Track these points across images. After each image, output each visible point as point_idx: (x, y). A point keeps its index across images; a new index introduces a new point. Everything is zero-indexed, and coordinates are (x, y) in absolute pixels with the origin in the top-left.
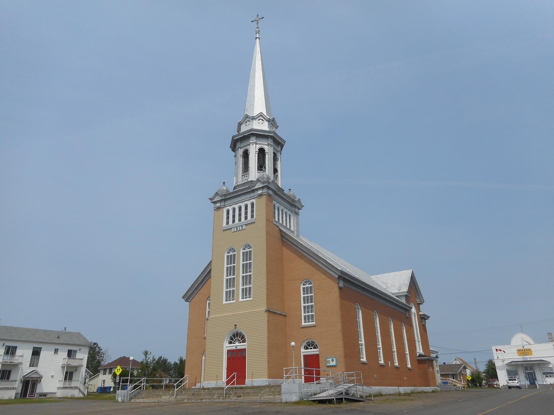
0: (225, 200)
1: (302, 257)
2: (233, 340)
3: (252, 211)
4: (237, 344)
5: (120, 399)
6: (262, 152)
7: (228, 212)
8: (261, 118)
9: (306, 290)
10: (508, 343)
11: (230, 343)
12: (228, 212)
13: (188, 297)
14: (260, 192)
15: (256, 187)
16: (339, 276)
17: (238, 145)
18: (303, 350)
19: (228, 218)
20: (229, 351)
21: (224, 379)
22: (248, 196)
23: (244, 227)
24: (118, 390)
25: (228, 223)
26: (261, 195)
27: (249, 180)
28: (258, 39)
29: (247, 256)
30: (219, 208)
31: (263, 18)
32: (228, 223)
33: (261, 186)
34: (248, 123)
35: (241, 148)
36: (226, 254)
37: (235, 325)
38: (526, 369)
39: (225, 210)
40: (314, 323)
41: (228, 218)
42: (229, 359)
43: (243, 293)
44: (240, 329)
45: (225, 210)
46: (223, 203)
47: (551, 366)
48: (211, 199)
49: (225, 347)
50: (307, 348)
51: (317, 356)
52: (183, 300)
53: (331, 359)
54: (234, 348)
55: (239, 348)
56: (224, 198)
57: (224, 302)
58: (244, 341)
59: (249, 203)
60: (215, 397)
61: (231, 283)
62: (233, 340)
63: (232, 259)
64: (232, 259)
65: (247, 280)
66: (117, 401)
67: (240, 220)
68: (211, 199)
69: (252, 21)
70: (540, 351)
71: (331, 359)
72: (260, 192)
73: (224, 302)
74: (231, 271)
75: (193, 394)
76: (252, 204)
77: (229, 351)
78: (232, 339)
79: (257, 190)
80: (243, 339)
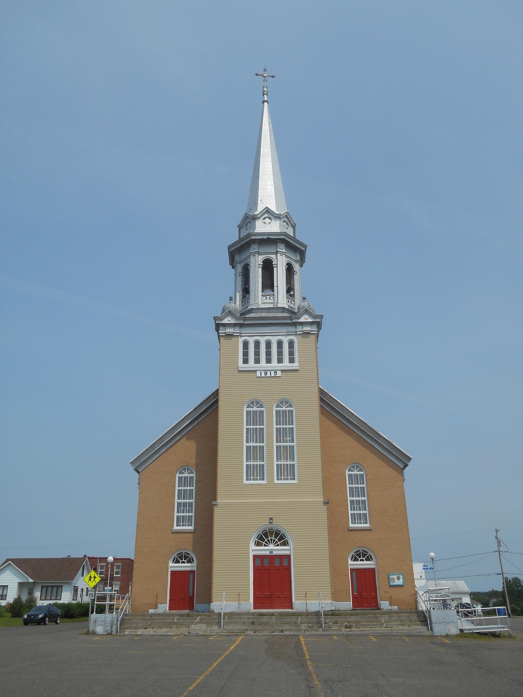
0: (241, 326)
1: (348, 431)
2: (263, 540)
3: (291, 353)
4: (271, 547)
5: (100, 630)
7: (246, 345)
8: (286, 219)
9: (353, 479)
11: (258, 544)
12: (246, 345)
13: (139, 465)
14: (307, 328)
15: (302, 320)
19: (246, 354)
20: (255, 557)
21: (252, 601)
22: (284, 330)
23: (279, 374)
24: (92, 613)
25: (246, 361)
26: (307, 334)
28: (266, 104)
29: (285, 417)
30: (229, 336)
31: (273, 77)
32: (246, 361)
33: (310, 320)
34: (267, 220)
35: (259, 253)
36: (245, 409)
37: (271, 519)
39: (241, 340)
40: (368, 525)
41: (246, 354)
42: (256, 569)
44: (279, 524)
45: (241, 340)
46: (237, 330)
48: (215, 319)
49: (251, 550)
50: (356, 560)
51: (372, 571)
52: (132, 468)
53: (395, 577)
54: (267, 553)
55: (275, 553)
56: (242, 322)
57: (245, 482)
58: (285, 544)
59: (286, 340)
60: (303, 627)
61: (255, 453)
62: (263, 540)
63: (255, 418)
64: (255, 418)
65: (286, 453)
66: (94, 633)
68: (215, 319)
69: (257, 75)
71: (395, 577)
72: (307, 328)
75: (253, 623)
76: (291, 344)
77: (255, 557)
78: (260, 538)
79: (302, 324)
80: (281, 538)
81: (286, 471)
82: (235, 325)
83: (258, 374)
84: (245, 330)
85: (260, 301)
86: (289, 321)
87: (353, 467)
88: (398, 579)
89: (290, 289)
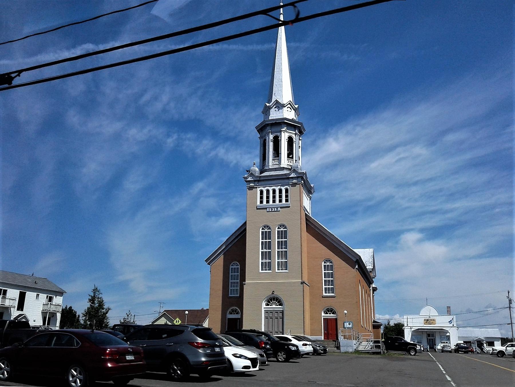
0: (259, 181)
6: (290, 141)
7: (262, 192)
8: (289, 106)
10: (418, 313)
11: (267, 305)
12: (262, 192)
16: (357, 260)
17: (268, 129)
18: (323, 314)
19: (261, 198)
25: (261, 202)
27: (281, 166)
29: (283, 235)
32: (261, 202)
38: (429, 335)
39: (258, 190)
41: (261, 198)
43: (278, 265)
44: (277, 294)
45: (258, 190)
47: (448, 334)
49: (263, 308)
50: (327, 313)
56: (258, 179)
61: (267, 255)
64: (267, 235)
67: (274, 201)
70: (442, 322)
73: (260, 271)
74: (268, 245)
81: (284, 265)
82: (255, 181)
83: (268, 209)
84: (260, 183)
85: (270, 164)
86: (285, 177)
87: (327, 261)
88: (349, 324)
89: (290, 154)
